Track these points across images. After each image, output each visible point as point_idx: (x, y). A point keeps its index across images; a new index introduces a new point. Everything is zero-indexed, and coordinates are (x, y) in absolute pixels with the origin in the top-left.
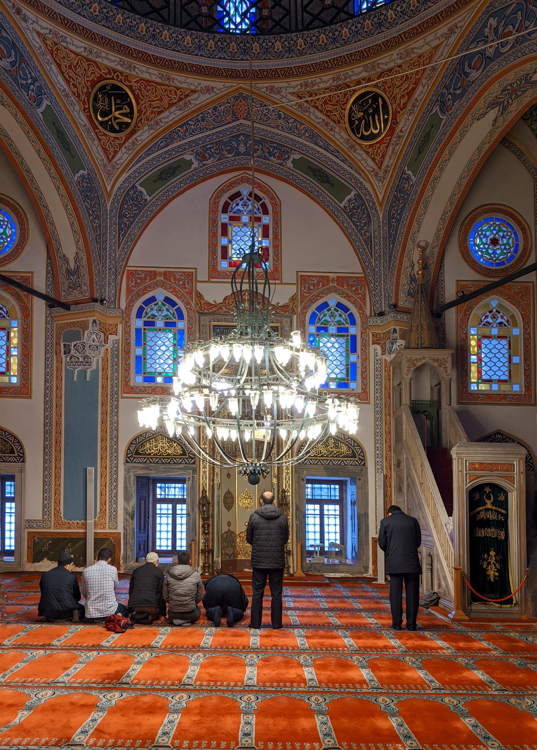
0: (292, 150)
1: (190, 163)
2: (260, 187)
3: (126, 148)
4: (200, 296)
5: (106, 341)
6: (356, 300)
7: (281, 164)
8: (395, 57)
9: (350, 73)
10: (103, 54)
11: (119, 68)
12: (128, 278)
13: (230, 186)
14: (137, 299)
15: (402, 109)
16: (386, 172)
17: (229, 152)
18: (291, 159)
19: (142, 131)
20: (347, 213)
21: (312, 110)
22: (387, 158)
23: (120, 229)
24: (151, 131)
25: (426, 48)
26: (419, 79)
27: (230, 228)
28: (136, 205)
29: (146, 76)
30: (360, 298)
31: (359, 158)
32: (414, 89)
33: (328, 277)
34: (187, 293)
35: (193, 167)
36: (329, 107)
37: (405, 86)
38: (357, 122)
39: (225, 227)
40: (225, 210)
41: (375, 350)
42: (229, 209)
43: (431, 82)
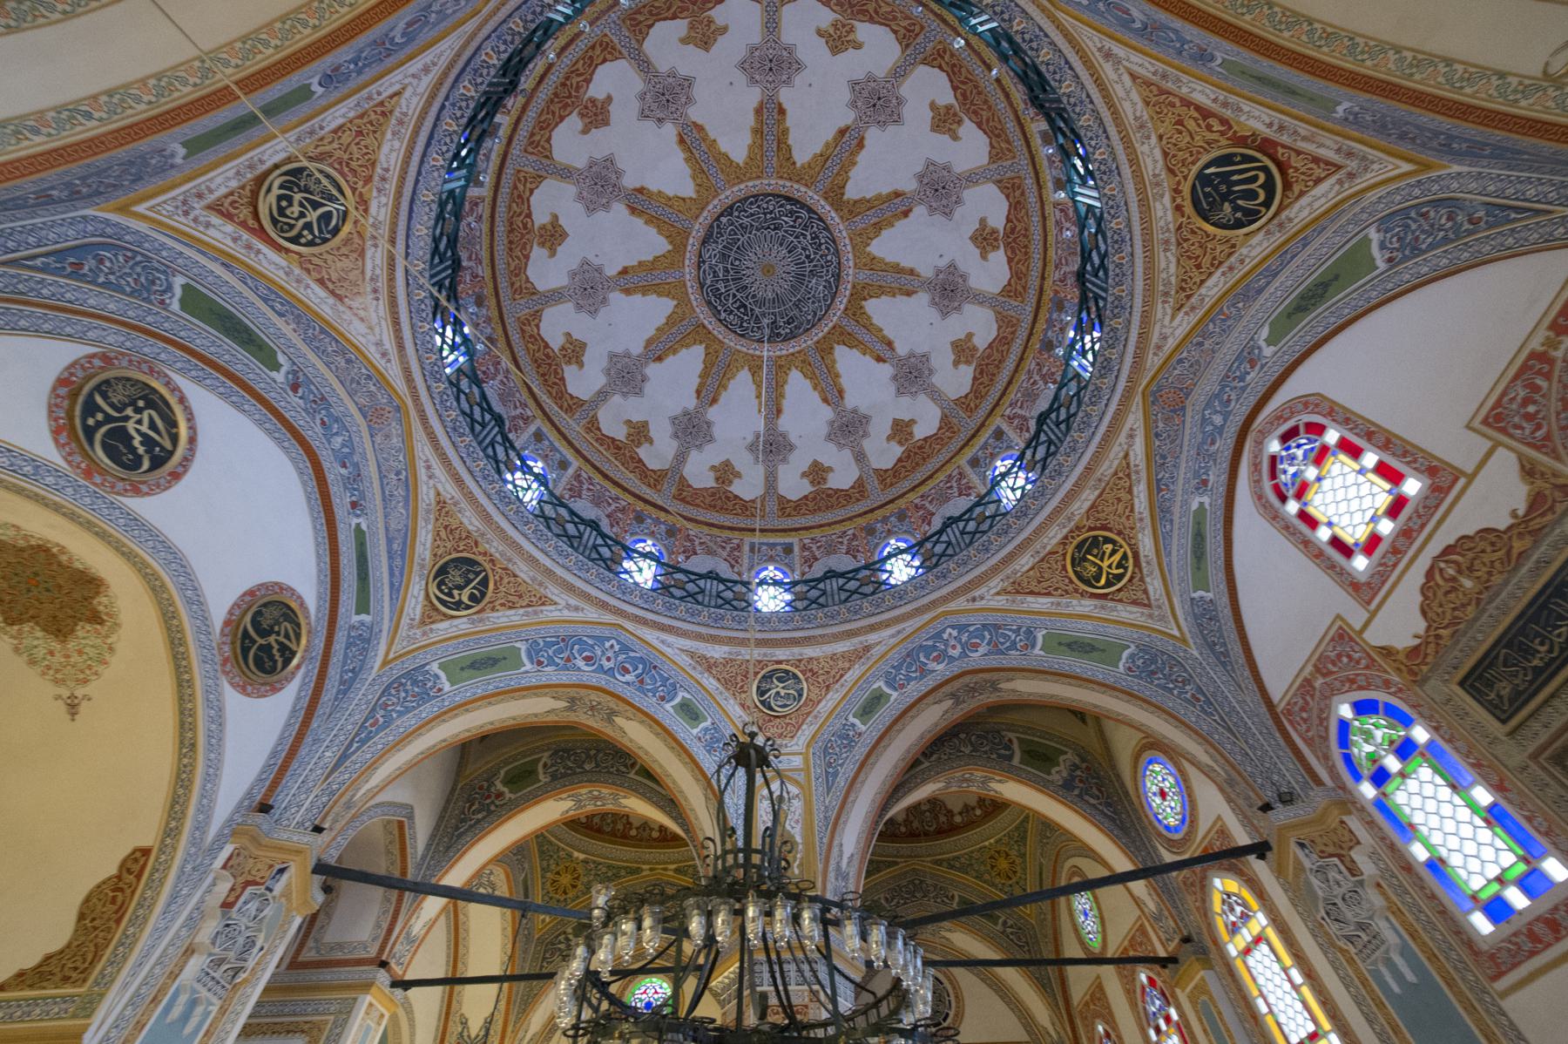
2: (1279, 418)
4: (1387, 652)
5: (1353, 870)
7: (1263, 366)
8: (1145, 148)
9: (1162, 223)
11: (1065, 531)
12: (1291, 722)
13: (1256, 467)
15: (1230, 127)
16: (1350, 154)
17: (1213, 443)
18: (1263, 344)
20: (1406, 259)
21: (1203, 291)
22: (1323, 152)
23: (1224, 664)
25: (1135, 96)
26: (1182, 99)
27: (1311, 510)
29: (1088, 504)
31: (1306, 212)
32: (1198, 108)
33: (1533, 355)
34: (1367, 667)
36: (1206, 262)
37: (1191, 124)
38: (1239, 215)
39: (1304, 516)
40: (1283, 499)
42: (1283, 489)
43: (1185, 78)
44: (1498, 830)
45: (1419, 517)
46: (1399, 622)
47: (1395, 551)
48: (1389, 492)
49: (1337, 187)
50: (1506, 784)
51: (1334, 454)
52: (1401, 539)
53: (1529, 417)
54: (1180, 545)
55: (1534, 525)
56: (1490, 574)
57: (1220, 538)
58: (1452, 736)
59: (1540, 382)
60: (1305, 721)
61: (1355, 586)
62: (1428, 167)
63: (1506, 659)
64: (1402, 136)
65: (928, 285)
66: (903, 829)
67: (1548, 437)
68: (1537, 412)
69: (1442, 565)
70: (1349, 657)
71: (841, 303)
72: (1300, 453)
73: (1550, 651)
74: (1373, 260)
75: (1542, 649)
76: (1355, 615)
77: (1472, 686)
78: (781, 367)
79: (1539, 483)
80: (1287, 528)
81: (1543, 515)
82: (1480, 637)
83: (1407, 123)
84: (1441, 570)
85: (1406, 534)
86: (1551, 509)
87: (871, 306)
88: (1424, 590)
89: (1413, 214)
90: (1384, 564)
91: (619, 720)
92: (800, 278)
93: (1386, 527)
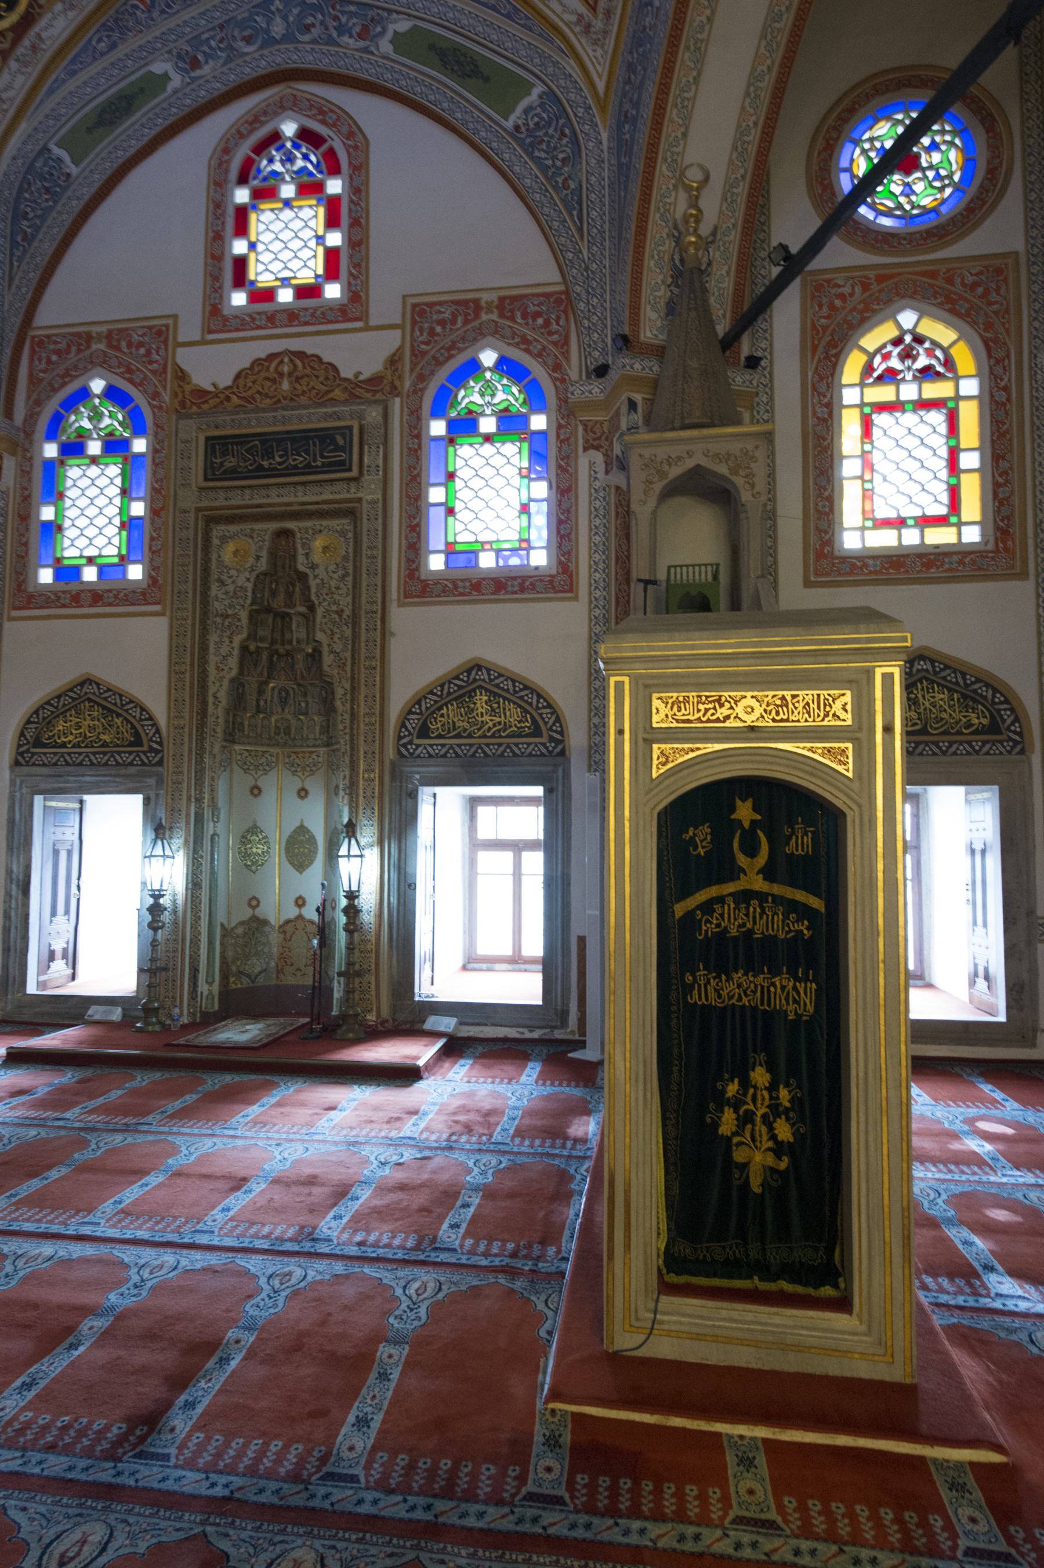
0: (390, 11)
1: (166, 77)
3: (18, 60)
4: (182, 376)
6: (544, 348)
7: (366, 50)
12: (33, 352)
13: (255, 120)
14: (49, 398)
16: (608, 13)
17: (248, 40)
18: (390, 34)
19: (49, 15)
20: (521, 142)
23: (14, 244)
24: (71, 14)
28: (47, 190)
30: (555, 344)
33: (476, 302)
34: (154, 372)
35: (170, 87)
40: (243, 180)
41: (592, 464)
42: (253, 172)
44: (124, 533)
45: (313, 315)
46: (213, 366)
47: (271, 319)
48: (317, 276)
49: (573, 18)
50: (162, 514)
51: (319, 201)
52: (285, 316)
53: (432, 332)
54: (93, 83)
55: (358, 392)
56: (304, 392)
57: (149, 134)
58: (162, 463)
59: (460, 320)
60: (49, 361)
61: (215, 313)
62: (603, 109)
63: (252, 448)
64: (631, 68)
66: (956, 696)
67: (424, 353)
68: (438, 334)
69: (286, 360)
70: (148, 353)
72: (300, 163)
73: (280, 464)
74: (513, 111)
75: (278, 459)
76: (190, 329)
77: (213, 445)
79: (389, 372)
80: (218, 205)
81: (367, 391)
82: (254, 423)
83: (645, 69)
84: (282, 362)
85: (290, 315)
86: (375, 392)
88: (257, 362)
89: (561, 121)
90: (253, 319)
93: (285, 296)
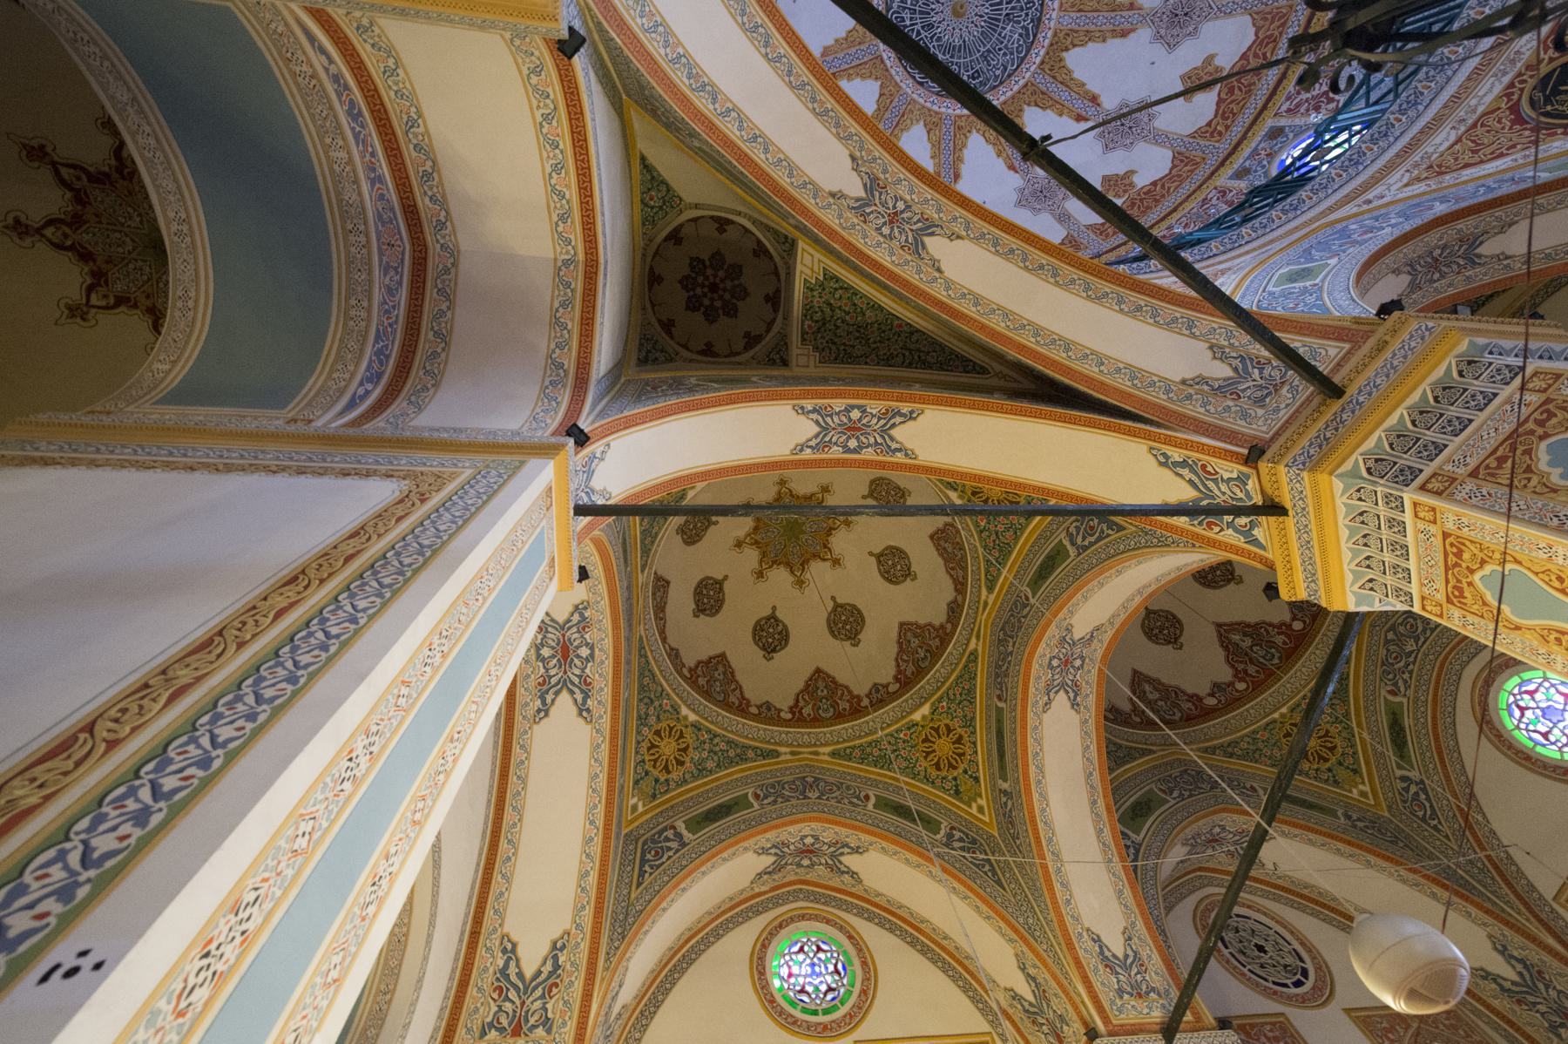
10: (1474, 102)
11: (1506, 79)
65: (1153, 17)
71: (1037, 55)
78: (960, 128)
87: (1073, 58)
91: (935, 245)
92: (993, 22)
